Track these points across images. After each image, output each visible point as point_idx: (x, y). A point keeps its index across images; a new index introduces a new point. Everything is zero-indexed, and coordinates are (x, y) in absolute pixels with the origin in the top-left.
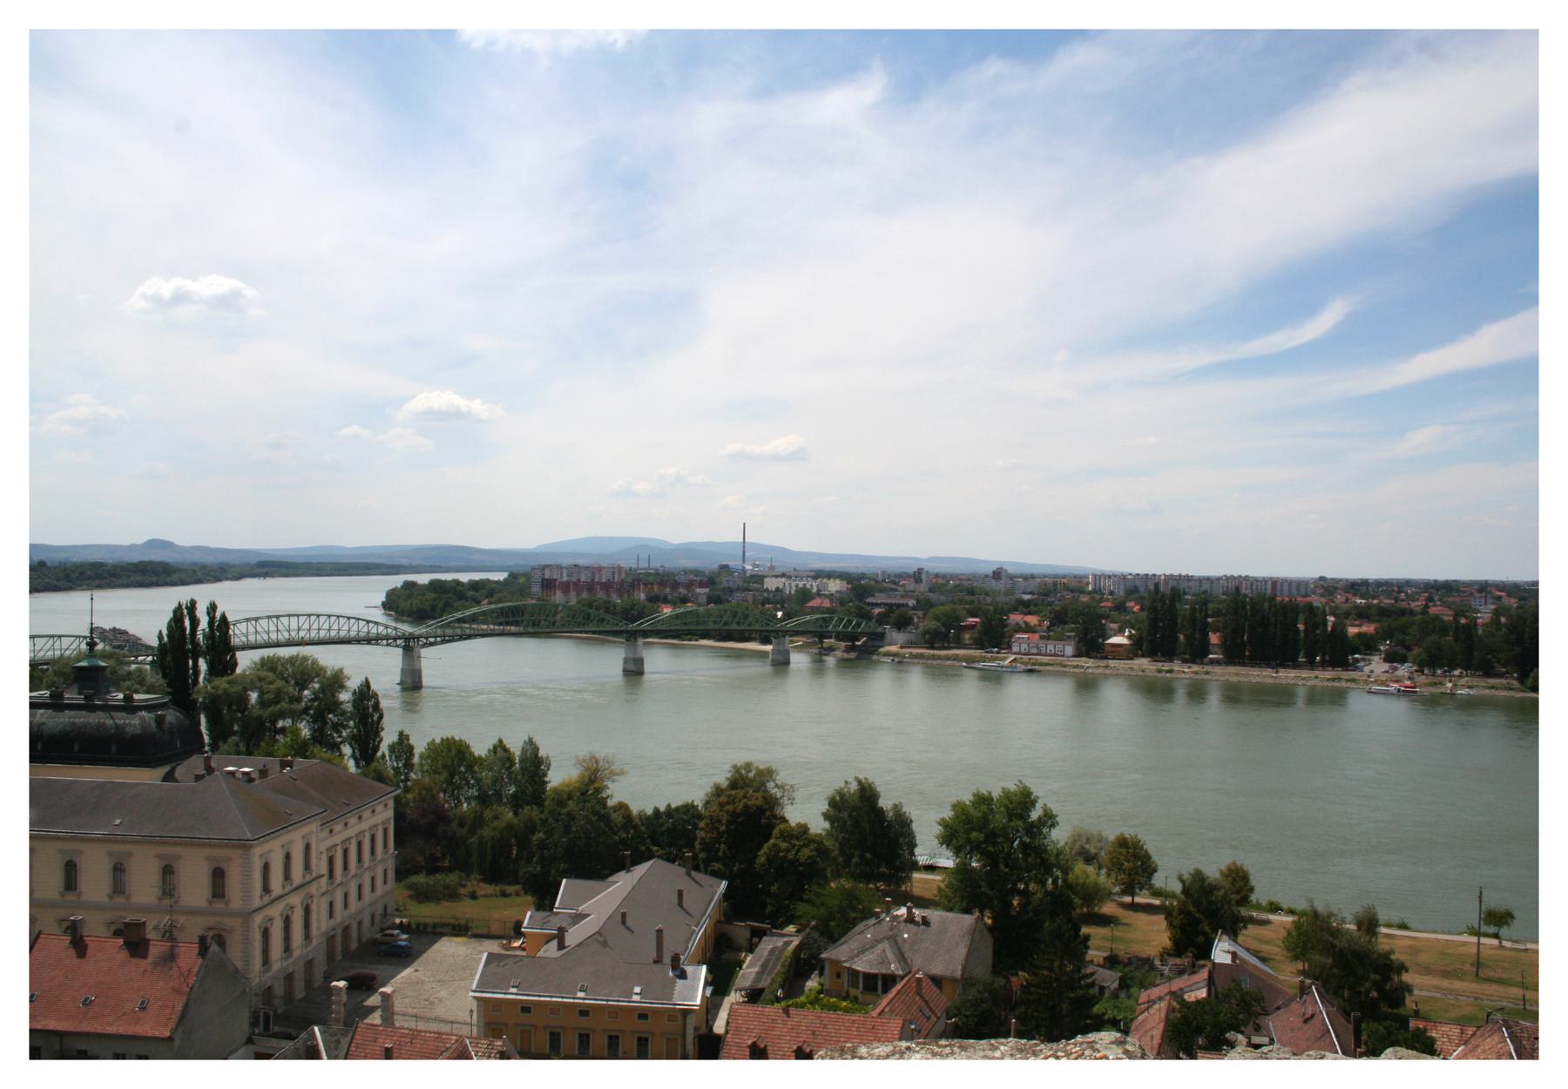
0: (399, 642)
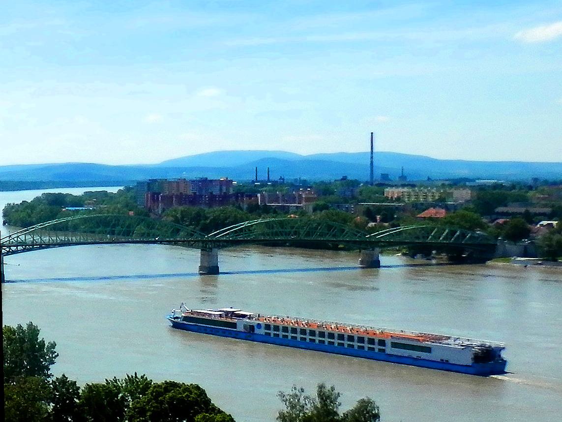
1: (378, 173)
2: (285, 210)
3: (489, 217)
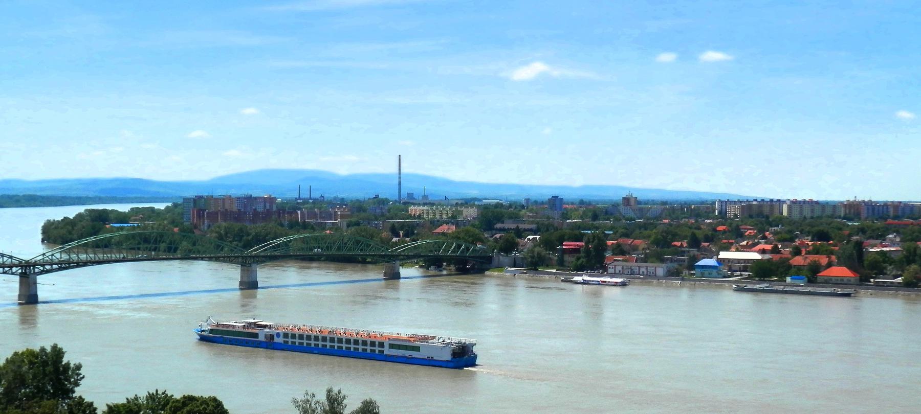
0: (14, 269)
1: (404, 192)
2: (323, 227)
3: (490, 232)
